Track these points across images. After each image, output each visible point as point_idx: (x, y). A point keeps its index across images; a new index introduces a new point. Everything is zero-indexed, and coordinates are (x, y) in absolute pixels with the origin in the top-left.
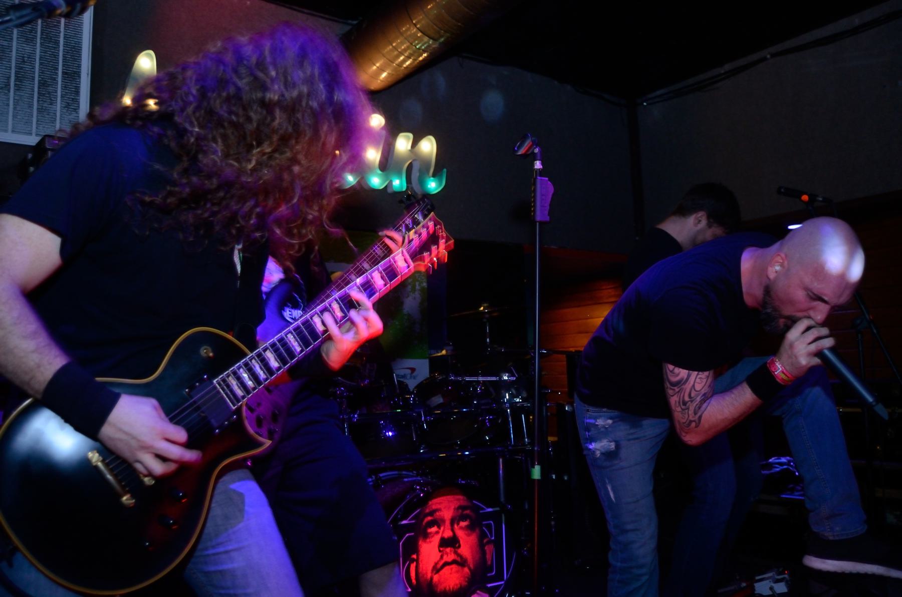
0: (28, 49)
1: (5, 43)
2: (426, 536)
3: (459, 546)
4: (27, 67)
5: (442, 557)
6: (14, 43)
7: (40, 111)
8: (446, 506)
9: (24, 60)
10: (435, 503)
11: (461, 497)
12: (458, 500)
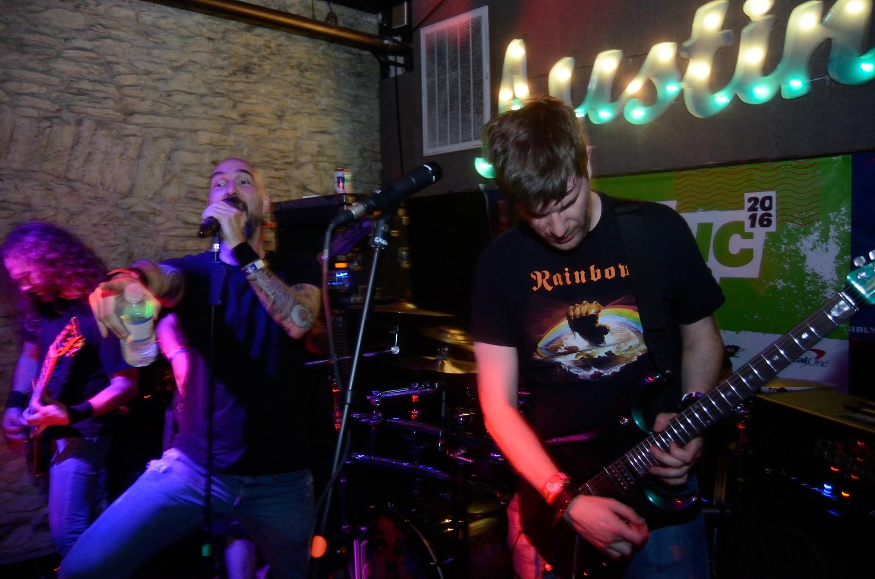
0: (454, 74)
1: (442, 77)
7: (463, 122)
9: (454, 85)
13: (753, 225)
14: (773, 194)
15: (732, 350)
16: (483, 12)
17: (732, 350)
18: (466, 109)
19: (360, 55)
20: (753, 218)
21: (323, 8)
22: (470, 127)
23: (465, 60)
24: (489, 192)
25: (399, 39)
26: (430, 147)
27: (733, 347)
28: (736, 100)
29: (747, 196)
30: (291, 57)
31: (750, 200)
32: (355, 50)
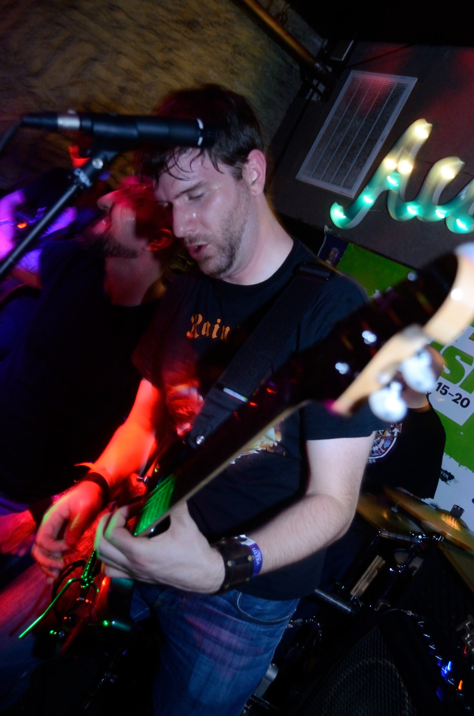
15: (447, 476)
16: (411, 83)
17: (447, 476)
18: (350, 156)
19: (292, 67)
21: (280, 4)
22: (345, 175)
23: (373, 116)
24: (330, 236)
25: (330, 69)
27: (449, 474)
30: (232, 35)
32: (290, 59)
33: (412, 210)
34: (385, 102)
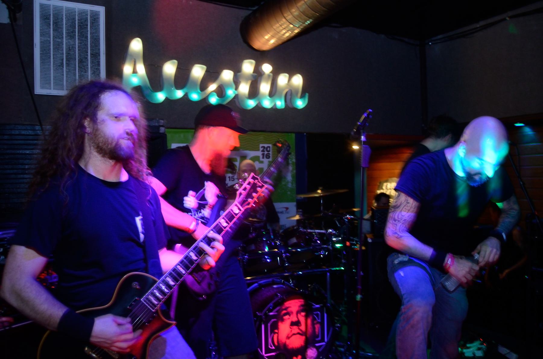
0: (71, 42)
1: (60, 40)
2: (283, 320)
3: (301, 325)
4: (72, 52)
5: (291, 331)
6: (64, 40)
8: (294, 305)
9: (70, 49)
10: (287, 304)
11: (302, 300)
12: (300, 302)
13: (263, 158)
14: (270, 145)
20: (263, 155)
23: (83, 36)
26: (42, 87)
28: (257, 105)
29: (261, 145)
31: (262, 147)
33: (160, 97)
34: (87, 25)
